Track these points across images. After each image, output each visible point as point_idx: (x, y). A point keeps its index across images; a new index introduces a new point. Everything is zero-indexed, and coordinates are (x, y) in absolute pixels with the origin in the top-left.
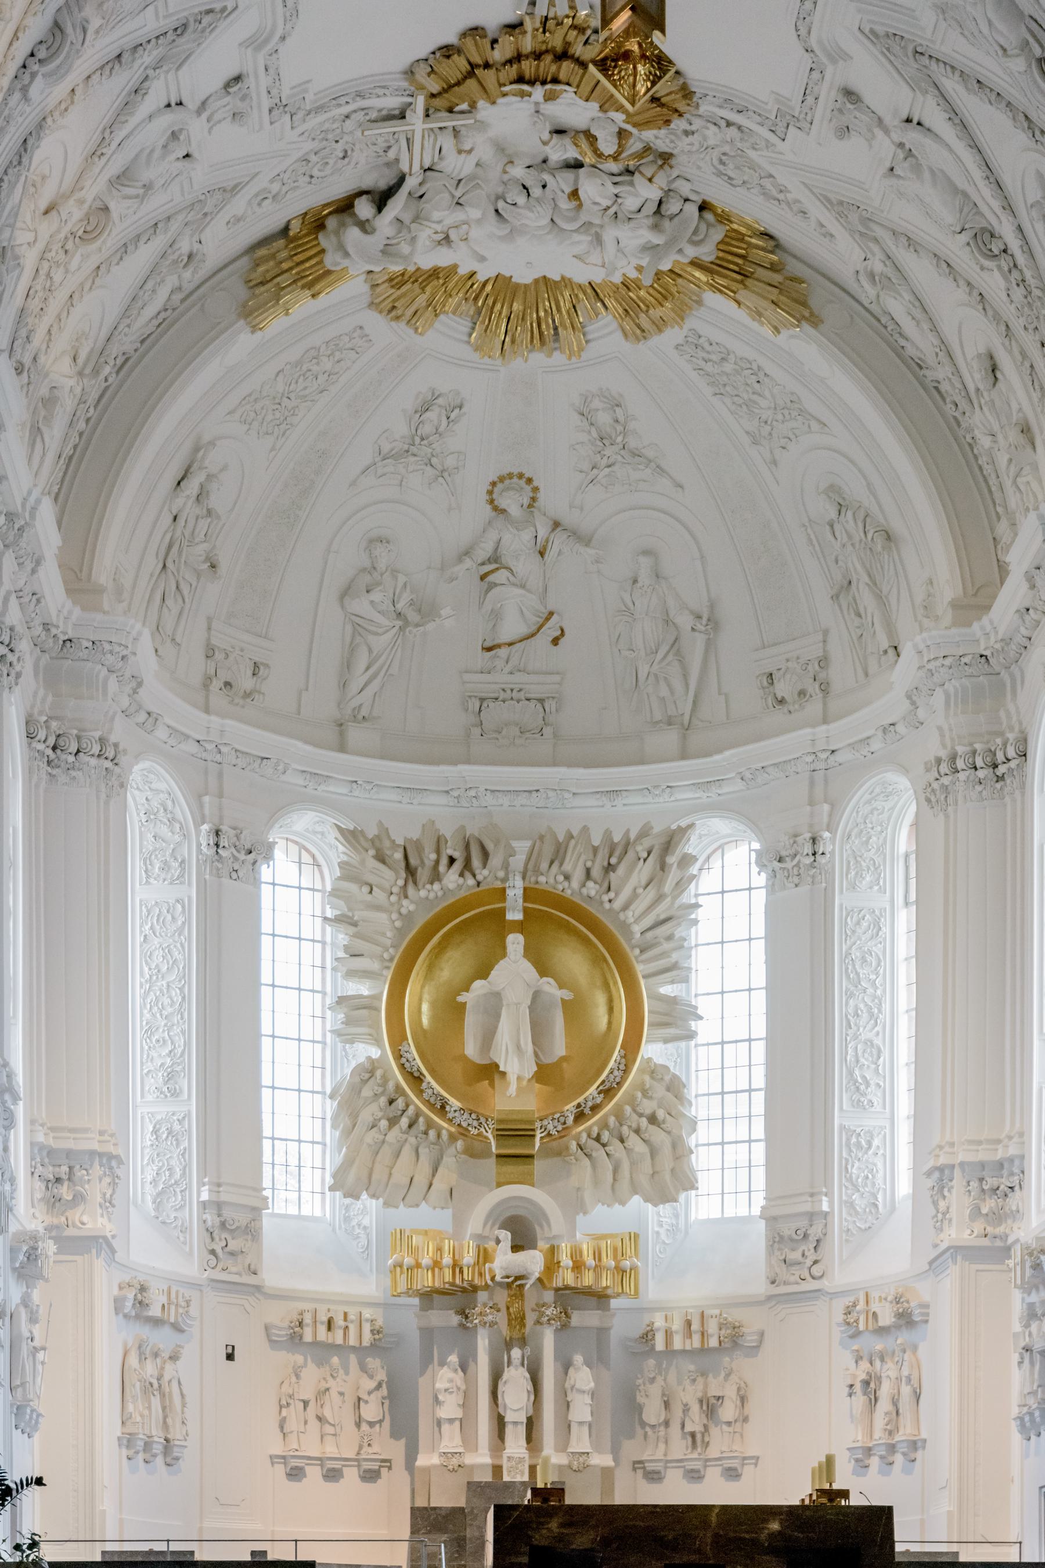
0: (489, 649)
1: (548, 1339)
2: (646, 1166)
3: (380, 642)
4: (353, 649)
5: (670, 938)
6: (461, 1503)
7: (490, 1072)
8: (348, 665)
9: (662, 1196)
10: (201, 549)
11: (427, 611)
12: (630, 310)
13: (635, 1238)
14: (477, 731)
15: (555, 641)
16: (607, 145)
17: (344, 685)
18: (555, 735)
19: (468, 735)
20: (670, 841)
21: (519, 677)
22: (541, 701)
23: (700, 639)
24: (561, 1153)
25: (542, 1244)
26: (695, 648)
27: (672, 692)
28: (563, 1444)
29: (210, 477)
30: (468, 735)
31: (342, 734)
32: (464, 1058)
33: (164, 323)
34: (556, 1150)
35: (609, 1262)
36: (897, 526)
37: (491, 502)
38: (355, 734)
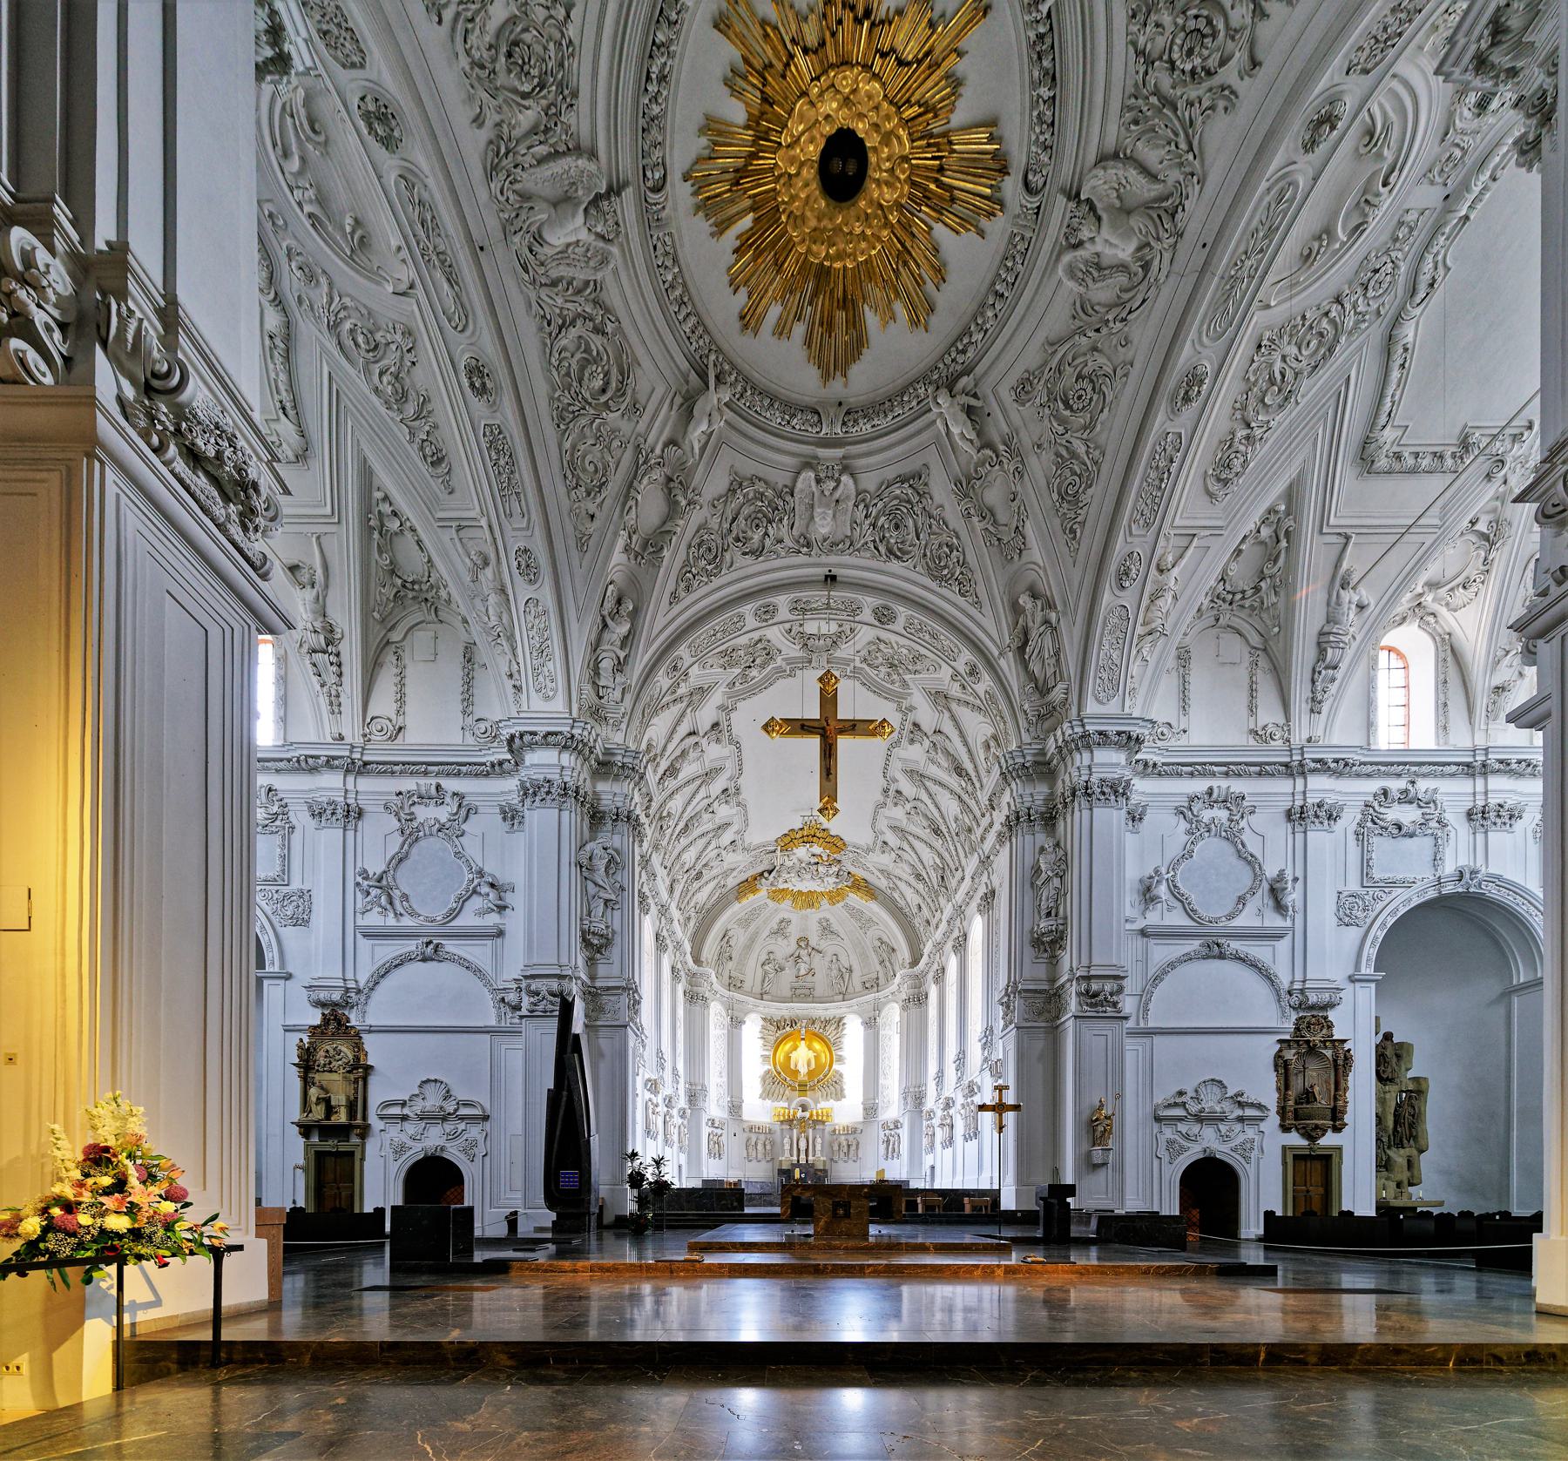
11: (782, 969)
16: (825, 858)
20: (841, 1019)
38: (765, 997)
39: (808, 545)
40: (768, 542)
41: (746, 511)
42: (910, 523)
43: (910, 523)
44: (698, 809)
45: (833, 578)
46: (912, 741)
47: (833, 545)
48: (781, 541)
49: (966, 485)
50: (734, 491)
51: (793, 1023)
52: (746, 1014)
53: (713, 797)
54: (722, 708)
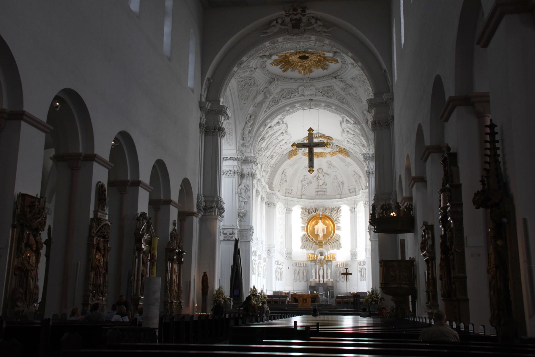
0: (318, 186)
1: (325, 266)
2: (336, 245)
3: (305, 186)
4: (303, 187)
5: (339, 219)
6: (315, 285)
7: (318, 235)
8: (302, 189)
9: (338, 249)
10: (285, 180)
12: (331, 154)
13: (335, 254)
14: (317, 195)
15: (326, 185)
17: (302, 191)
18: (326, 196)
19: (316, 196)
21: (322, 189)
22: (324, 192)
23: (342, 185)
24: (326, 244)
25: (324, 255)
26: (341, 186)
27: (339, 190)
28: (327, 278)
29: (286, 172)
30: (316, 196)
31: (301, 197)
32: (315, 234)
33: (280, 160)
34: (325, 244)
35: (331, 257)
36: (361, 175)
37: (317, 170)
39: (304, 96)
40: (292, 97)
41: (286, 93)
42: (331, 93)
43: (331, 93)
44: (272, 141)
45: (312, 99)
46: (347, 123)
47: (311, 95)
48: (296, 96)
49: (344, 90)
50: (282, 91)
51: (316, 210)
52: (294, 205)
53: (277, 136)
54: (280, 119)
